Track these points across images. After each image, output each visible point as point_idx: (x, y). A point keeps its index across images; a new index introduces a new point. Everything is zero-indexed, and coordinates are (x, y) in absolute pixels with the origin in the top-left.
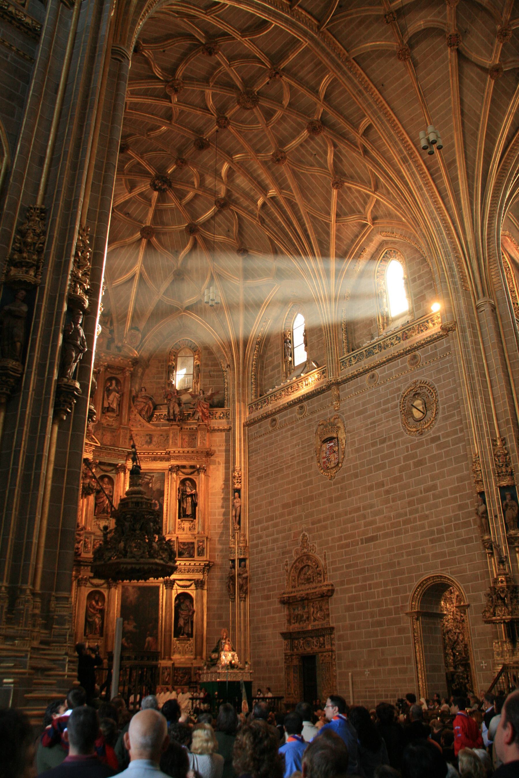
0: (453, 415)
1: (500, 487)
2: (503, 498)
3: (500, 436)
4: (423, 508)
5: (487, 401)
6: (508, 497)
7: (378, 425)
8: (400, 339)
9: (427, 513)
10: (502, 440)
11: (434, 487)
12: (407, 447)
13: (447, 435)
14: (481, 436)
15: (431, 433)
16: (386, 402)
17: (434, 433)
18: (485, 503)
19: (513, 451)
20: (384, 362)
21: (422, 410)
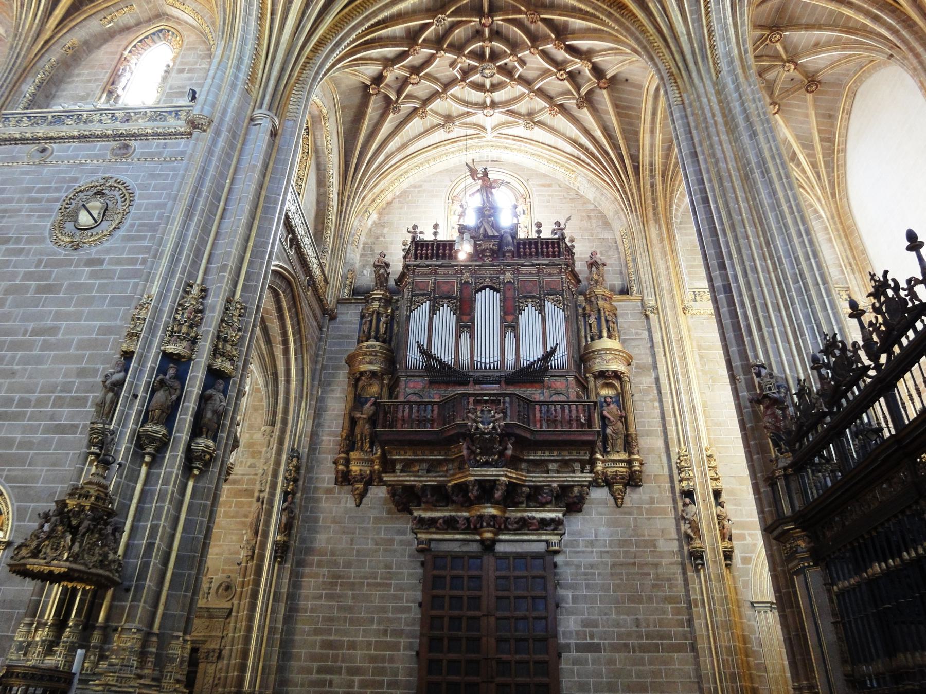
0: (144, 238)
1: (164, 352)
2: (162, 370)
3: (202, 284)
4: (13, 358)
5: (206, 230)
6: (171, 372)
7: (10, 217)
8: (117, 119)
9: (16, 367)
10: (202, 291)
11: (53, 331)
12: (40, 261)
13: (119, 262)
14: (171, 272)
15: (93, 252)
16: (46, 190)
17: (97, 252)
18: (126, 371)
19: (213, 310)
20: (73, 137)
21: (96, 216)
